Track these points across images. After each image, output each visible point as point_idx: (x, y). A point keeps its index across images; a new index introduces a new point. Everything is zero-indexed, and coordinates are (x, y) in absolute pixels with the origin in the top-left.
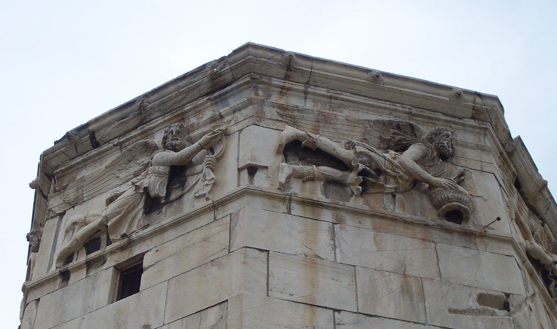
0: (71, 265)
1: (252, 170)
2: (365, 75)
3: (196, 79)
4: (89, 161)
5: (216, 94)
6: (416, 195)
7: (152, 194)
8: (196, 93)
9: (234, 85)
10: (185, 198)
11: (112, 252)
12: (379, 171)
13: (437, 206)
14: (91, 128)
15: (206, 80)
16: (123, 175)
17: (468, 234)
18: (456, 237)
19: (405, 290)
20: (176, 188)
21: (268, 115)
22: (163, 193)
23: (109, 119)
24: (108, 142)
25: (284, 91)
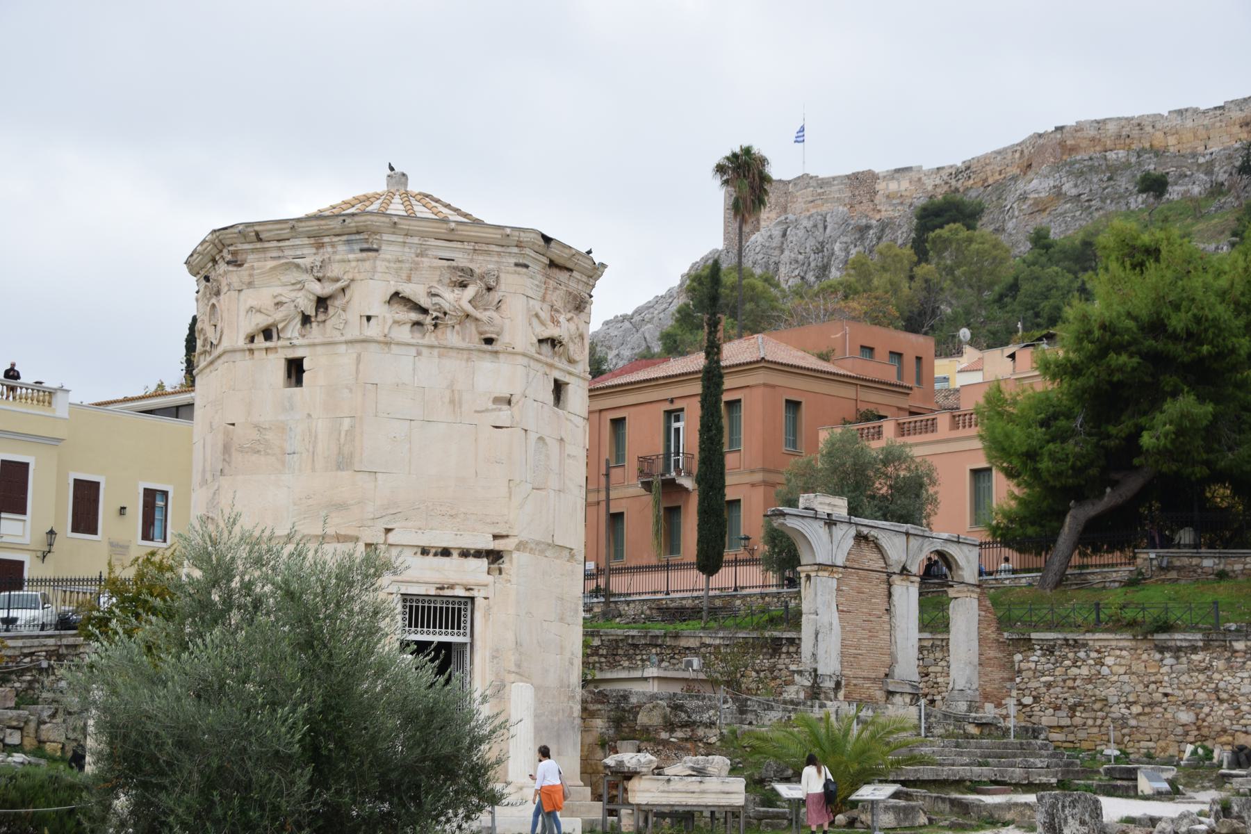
0: (253, 346)
1: (369, 318)
6: (468, 323)
11: (283, 347)
12: (445, 314)
14: (257, 228)
16: (284, 279)
17: (496, 352)
18: (488, 356)
19: (452, 402)
21: (379, 269)
22: (313, 314)
23: (270, 227)
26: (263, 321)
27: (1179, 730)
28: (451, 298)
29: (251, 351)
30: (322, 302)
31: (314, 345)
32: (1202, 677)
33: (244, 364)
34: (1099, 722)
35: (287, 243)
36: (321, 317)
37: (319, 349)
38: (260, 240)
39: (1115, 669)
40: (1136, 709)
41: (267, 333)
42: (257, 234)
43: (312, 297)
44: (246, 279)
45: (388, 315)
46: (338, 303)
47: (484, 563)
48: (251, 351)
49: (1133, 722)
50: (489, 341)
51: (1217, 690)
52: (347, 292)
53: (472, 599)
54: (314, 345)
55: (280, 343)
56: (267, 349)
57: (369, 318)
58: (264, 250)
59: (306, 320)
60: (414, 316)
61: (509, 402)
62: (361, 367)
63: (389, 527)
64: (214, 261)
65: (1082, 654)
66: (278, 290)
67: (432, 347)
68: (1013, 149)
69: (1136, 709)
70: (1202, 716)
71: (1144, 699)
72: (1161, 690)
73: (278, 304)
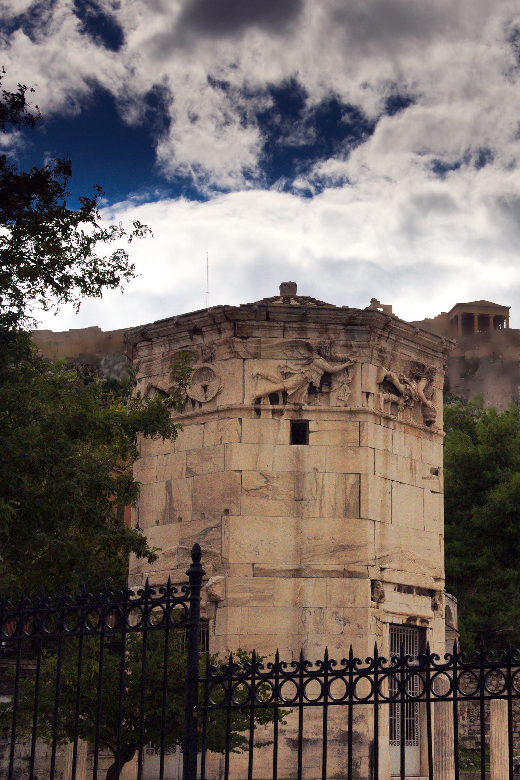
1: (368, 394)
2: (412, 329)
3: (341, 314)
4: (262, 327)
5: (349, 327)
7: (314, 384)
8: (338, 321)
9: (361, 328)
10: (331, 394)
12: (411, 398)
13: (425, 416)
14: (270, 309)
15: (347, 318)
16: (289, 353)
17: (432, 433)
19: (411, 468)
20: (326, 385)
24: (277, 321)
25: (381, 336)
26: (272, 388)
29: (258, 412)
30: (327, 378)
31: (320, 411)
33: (249, 423)
35: (294, 325)
36: (325, 389)
37: (323, 416)
41: (273, 397)
43: (321, 372)
44: (252, 350)
45: (381, 394)
46: (340, 379)
47: (427, 601)
48: (258, 412)
52: (350, 371)
54: (320, 411)
55: (287, 407)
56: (274, 412)
57: (368, 394)
58: (271, 328)
59: (312, 390)
60: (394, 397)
62: (364, 433)
63: (383, 566)
66: (283, 363)
67: (401, 423)
73: (287, 375)
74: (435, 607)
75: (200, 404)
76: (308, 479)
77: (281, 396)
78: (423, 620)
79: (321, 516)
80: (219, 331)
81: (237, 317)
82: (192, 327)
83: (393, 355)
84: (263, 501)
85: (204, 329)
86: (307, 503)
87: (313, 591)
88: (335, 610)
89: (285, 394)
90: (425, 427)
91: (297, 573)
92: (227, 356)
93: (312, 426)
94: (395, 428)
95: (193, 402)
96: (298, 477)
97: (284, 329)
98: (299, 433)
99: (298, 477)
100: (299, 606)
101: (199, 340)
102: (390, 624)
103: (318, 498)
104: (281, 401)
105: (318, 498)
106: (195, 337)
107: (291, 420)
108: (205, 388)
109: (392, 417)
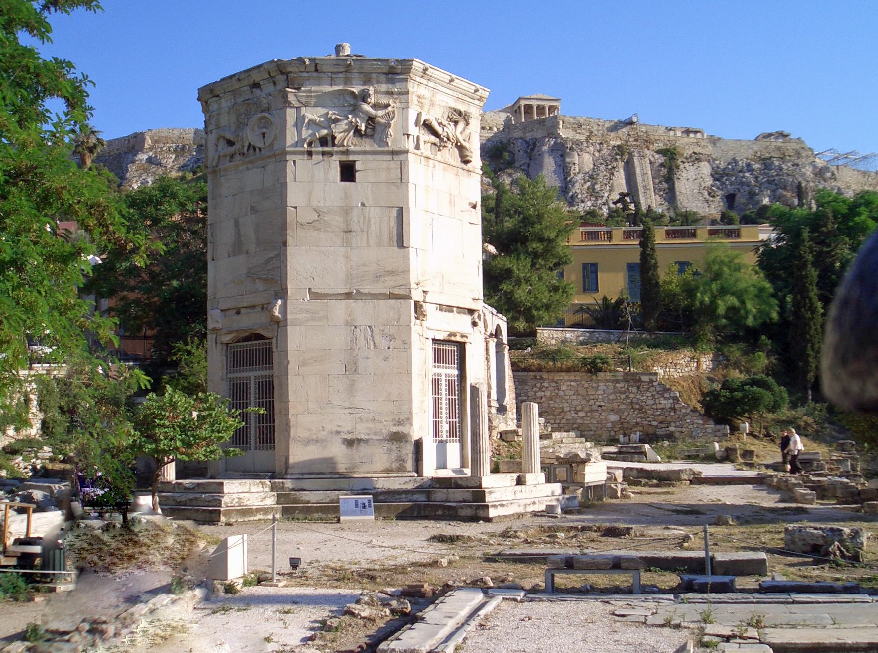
1: (408, 135)
5: (390, 76)
8: (380, 71)
11: (337, 153)
12: (449, 139)
14: (317, 62)
19: (450, 202)
27: (609, 425)
28: (450, 129)
29: (310, 154)
32: (623, 396)
34: (557, 422)
35: (340, 75)
38: (317, 70)
39: (567, 393)
40: (581, 414)
41: (324, 142)
42: (316, 65)
47: (468, 319)
48: (310, 154)
49: (579, 421)
50: (466, 162)
51: (632, 403)
53: (464, 343)
56: (324, 153)
60: (433, 139)
61: (474, 207)
64: (257, 85)
65: (545, 384)
68: (124, 139)
69: (581, 414)
70: (623, 417)
71: (587, 409)
72: (597, 403)
74: (474, 324)
75: (260, 149)
76: (355, 213)
77: (329, 138)
78: (462, 336)
79: (368, 245)
80: (275, 83)
81: (289, 70)
82: (251, 82)
83: (431, 100)
84: (315, 233)
85: (262, 83)
86: (354, 234)
87: (362, 311)
88: (382, 328)
89: (334, 138)
90: (463, 165)
91: (348, 296)
92: (281, 106)
93: (358, 166)
94: (434, 166)
95: (255, 149)
96: (347, 211)
97: (332, 79)
98: (348, 172)
99: (347, 211)
100: (351, 325)
101: (257, 92)
102: (433, 340)
103: (365, 230)
104: (330, 143)
105: (365, 230)
106: (254, 90)
107: (340, 161)
108: (264, 134)
109: (431, 156)
